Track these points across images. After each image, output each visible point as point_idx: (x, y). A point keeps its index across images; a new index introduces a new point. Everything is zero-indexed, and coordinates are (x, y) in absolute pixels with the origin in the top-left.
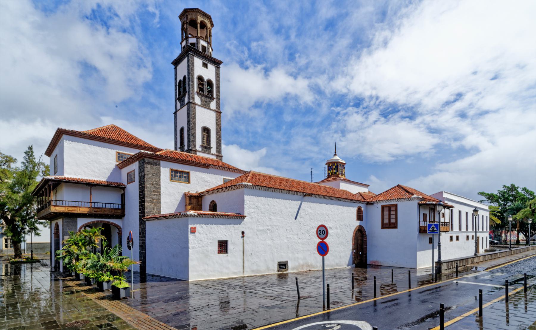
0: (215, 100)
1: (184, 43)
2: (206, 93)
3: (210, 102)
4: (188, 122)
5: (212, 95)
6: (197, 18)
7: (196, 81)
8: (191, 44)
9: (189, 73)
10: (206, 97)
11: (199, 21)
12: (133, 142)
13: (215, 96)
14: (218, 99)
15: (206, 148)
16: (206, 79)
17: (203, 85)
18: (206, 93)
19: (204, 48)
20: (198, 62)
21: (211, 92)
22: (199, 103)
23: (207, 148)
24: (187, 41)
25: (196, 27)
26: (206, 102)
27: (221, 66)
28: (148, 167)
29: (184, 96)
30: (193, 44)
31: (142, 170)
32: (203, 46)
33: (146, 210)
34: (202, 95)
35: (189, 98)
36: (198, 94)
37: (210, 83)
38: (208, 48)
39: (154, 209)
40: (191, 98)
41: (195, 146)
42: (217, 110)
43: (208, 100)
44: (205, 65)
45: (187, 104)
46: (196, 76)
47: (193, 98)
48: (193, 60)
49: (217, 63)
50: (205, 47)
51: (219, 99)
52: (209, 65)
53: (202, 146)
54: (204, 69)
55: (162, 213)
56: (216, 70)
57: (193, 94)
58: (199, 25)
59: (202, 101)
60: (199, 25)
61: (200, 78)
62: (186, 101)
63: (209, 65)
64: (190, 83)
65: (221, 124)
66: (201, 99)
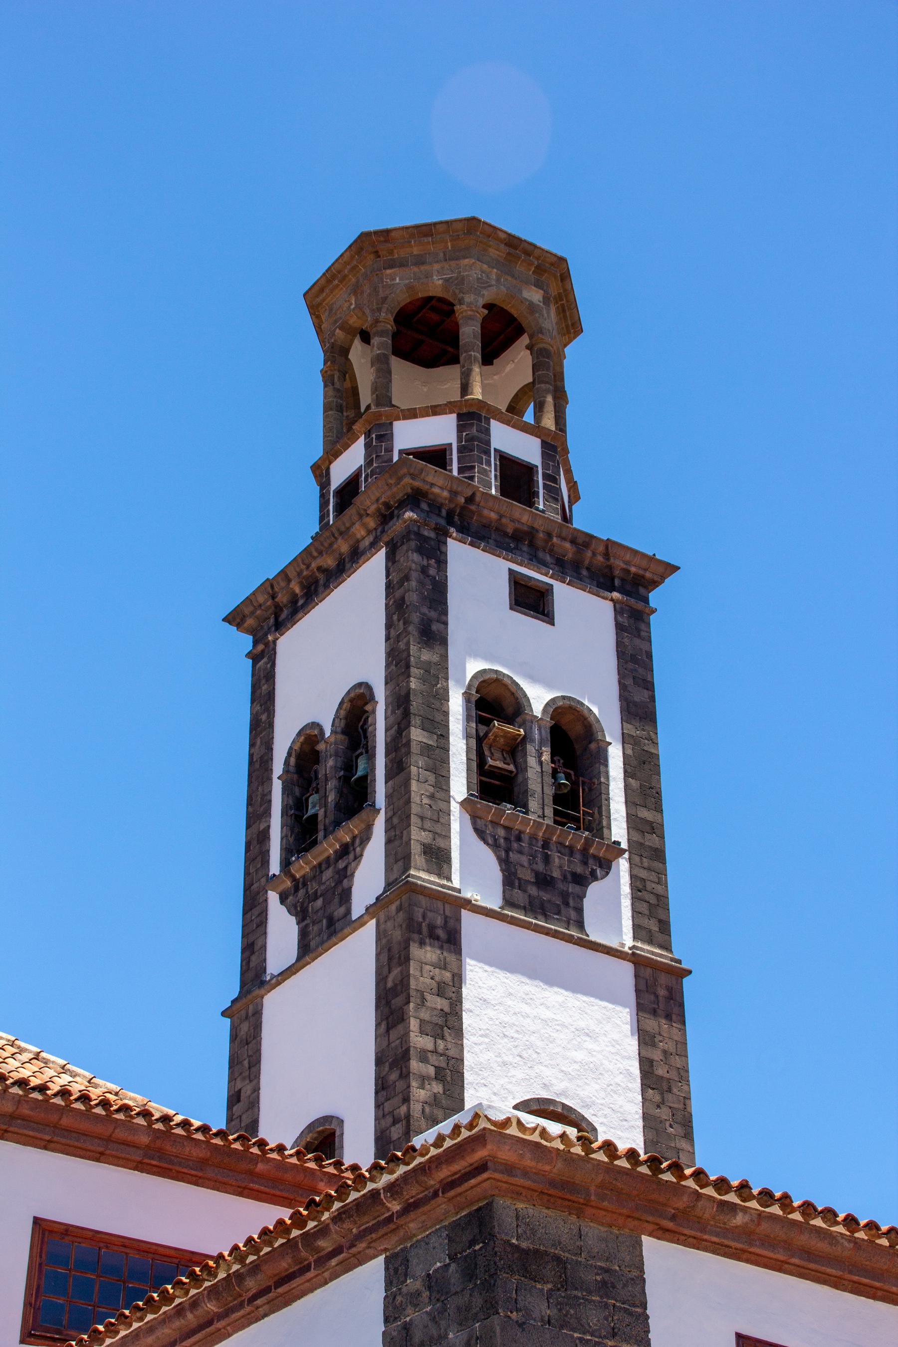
0: (623, 865)
1: (351, 460)
3: (582, 881)
4: (392, 1064)
5: (598, 825)
9: (397, 662)
13: (619, 830)
14: (649, 851)
16: (538, 698)
17: (515, 749)
20: (475, 576)
21: (578, 798)
24: (380, 437)
26: (544, 881)
27: (655, 597)
29: (350, 853)
30: (436, 456)
32: (507, 463)
35: (398, 857)
38: (552, 479)
40: (418, 858)
42: (647, 950)
44: (531, 600)
45: (370, 911)
47: (439, 858)
49: (628, 582)
50: (529, 469)
51: (659, 855)
57: (439, 818)
59: (510, 880)
62: (369, 879)
63: (566, 596)
64: (417, 735)
65: (683, 1074)
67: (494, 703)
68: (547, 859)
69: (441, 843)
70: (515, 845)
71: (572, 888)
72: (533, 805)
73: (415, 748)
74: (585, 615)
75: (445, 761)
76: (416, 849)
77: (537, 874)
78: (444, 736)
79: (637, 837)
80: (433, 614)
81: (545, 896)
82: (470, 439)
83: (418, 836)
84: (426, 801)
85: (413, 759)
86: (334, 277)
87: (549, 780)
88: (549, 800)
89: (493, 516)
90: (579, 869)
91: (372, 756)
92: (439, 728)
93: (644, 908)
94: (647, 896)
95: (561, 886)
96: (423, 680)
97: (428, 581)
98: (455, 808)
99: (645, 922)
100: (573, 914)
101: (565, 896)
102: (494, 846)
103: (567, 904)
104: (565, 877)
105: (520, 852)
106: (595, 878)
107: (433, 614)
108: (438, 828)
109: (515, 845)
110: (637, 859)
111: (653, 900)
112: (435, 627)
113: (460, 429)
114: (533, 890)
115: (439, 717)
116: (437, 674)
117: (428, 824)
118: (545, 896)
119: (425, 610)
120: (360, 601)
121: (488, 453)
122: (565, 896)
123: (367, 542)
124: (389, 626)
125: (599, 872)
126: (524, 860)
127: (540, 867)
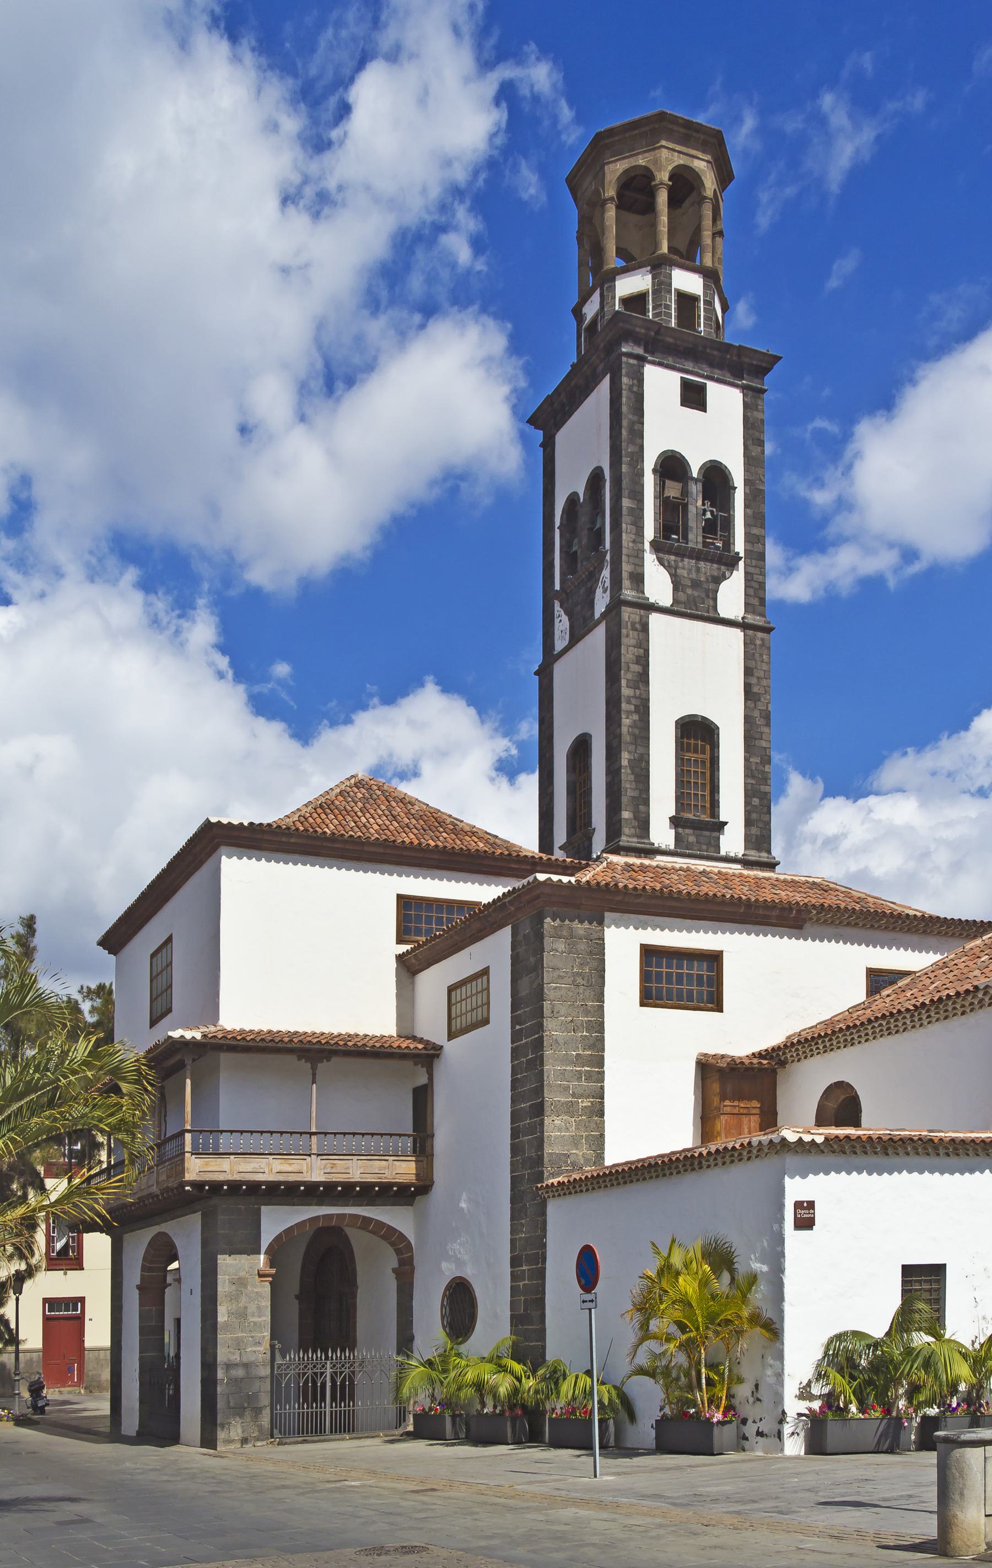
2: (695, 539)
5: (728, 542)
6: (656, 161)
8: (626, 301)
10: (697, 556)
11: (663, 176)
12: (445, 840)
15: (697, 826)
18: (695, 539)
22: (666, 599)
23: (699, 825)
25: (650, 208)
28: (556, 952)
31: (527, 965)
33: (548, 1150)
34: (681, 553)
39: (575, 1142)
41: (644, 825)
53: (675, 822)
55: (608, 1162)
58: (662, 198)
60: (662, 198)
67: (672, 466)
68: (698, 570)
70: (680, 564)
71: (711, 586)
77: (692, 580)
81: (696, 594)
82: (660, 283)
89: (671, 340)
95: (705, 586)
100: (711, 603)
103: (708, 596)
104: (707, 580)
105: (683, 568)
106: (725, 578)
113: (653, 278)
114: (689, 591)
118: (696, 594)
122: (707, 591)
125: (727, 574)
127: (694, 576)
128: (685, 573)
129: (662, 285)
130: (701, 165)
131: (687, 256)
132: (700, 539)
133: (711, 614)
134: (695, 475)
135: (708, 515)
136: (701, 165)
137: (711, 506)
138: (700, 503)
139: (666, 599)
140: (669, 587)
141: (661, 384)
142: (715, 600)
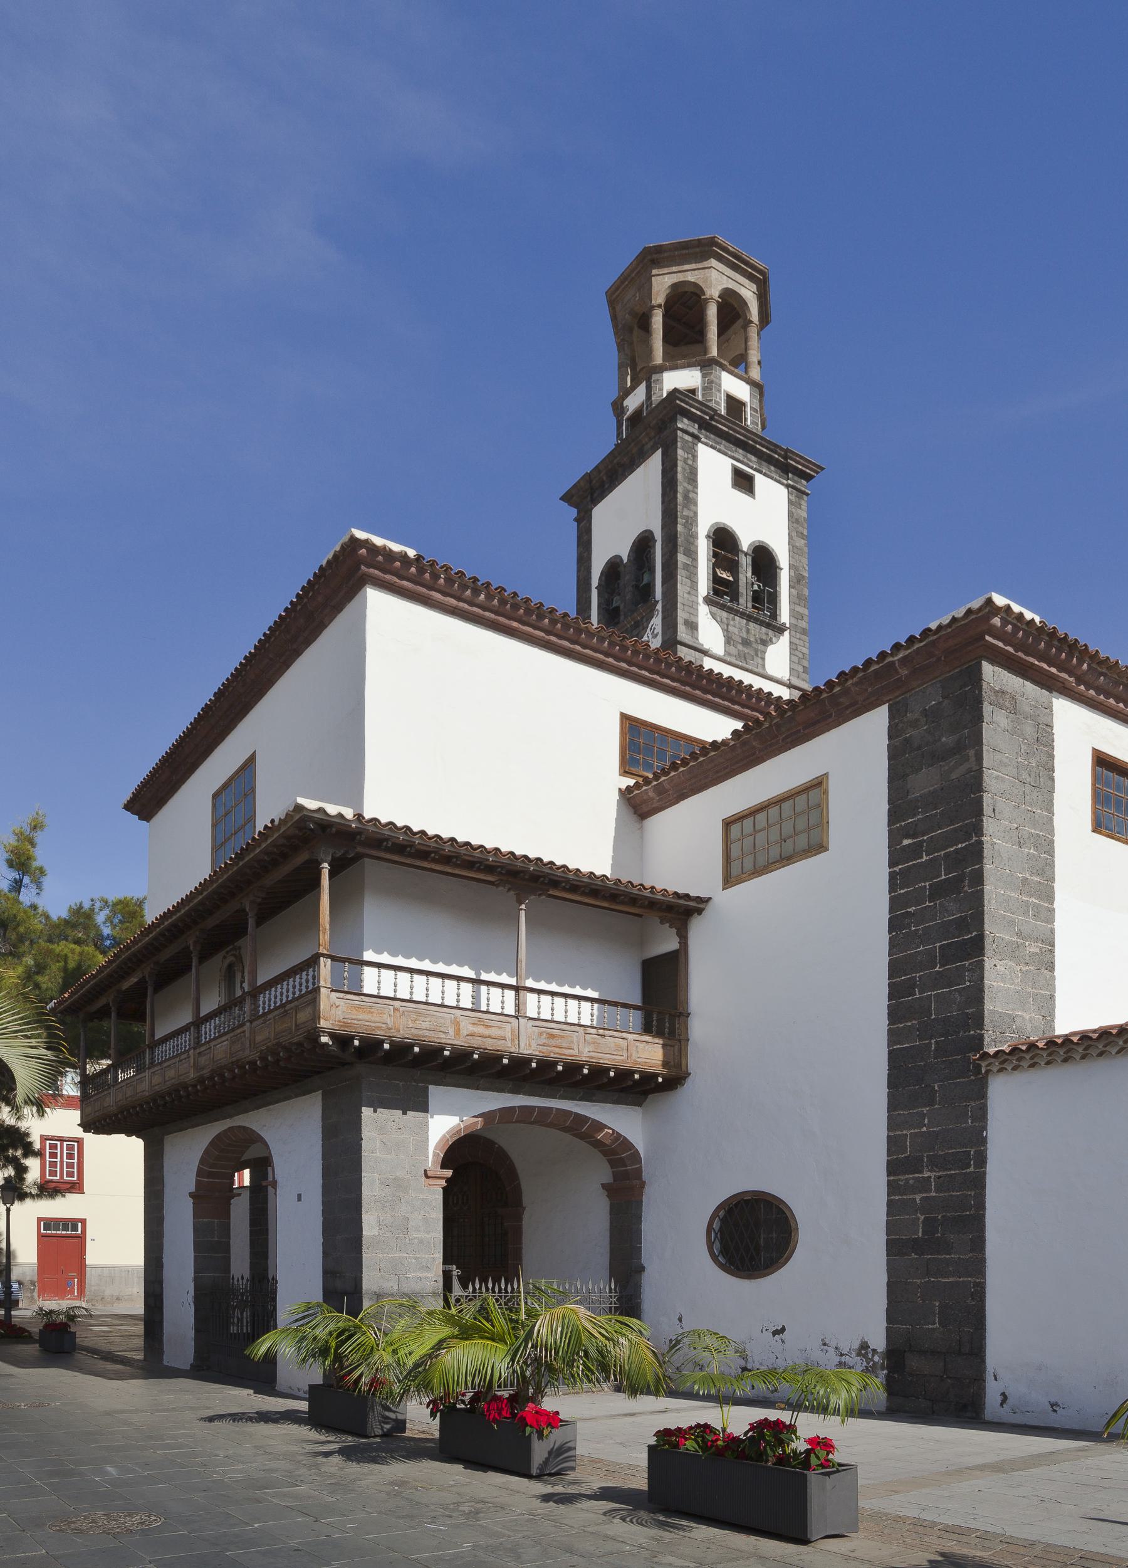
2: (745, 602)
3: (765, 643)
5: (774, 615)
7: (703, 548)
13: (784, 617)
17: (733, 567)
19: (735, 405)
20: (713, 466)
21: (765, 599)
22: (719, 650)
26: (746, 643)
32: (730, 399)
36: (708, 601)
37: (763, 558)
40: (681, 628)
43: (757, 631)
46: (703, 529)
47: (693, 626)
48: (695, 457)
50: (743, 404)
52: (760, 481)
54: (741, 497)
56: (790, 502)
59: (729, 640)
61: (723, 539)
64: (681, 558)
66: (726, 631)
68: (748, 631)
69: (693, 619)
70: (732, 623)
71: (760, 647)
72: (742, 600)
73: (680, 565)
74: (772, 493)
75: (696, 574)
76: (680, 621)
77: (743, 639)
78: (695, 560)
79: (794, 621)
80: (690, 487)
83: (681, 615)
84: (686, 595)
85: (679, 571)
86: (625, 279)
87: (749, 586)
88: (750, 599)
90: (764, 637)
91: (652, 570)
92: (692, 554)
93: (796, 659)
94: (797, 653)
95: (754, 645)
96: (684, 525)
97: (687, 467)
98: (701, 600)
99: (796, 667)
100: (760, 661)
101: (756, 651)
102: (720, 622)
103: (757, 655)
107: (690, 487)
108: (691, 611)
109: (732, 623)
110: (793, 633)
111: (801, 655)
112: (691, 495)
113: (704, 376)
114: (740, 647)
115: (692, 548)
116: (692, 521)
117: (686, 608)
119: (686, 485)
120: (647, 477)
121: (720, 391)
122: (756, 651)
123: (649, 446)
124: (664, 495)
125: (774, 640)
126: (736, 631)
127: (744, 635)
128: (736, 631)
129: (710, 386)
130: (748, 292)
131: (738, 363)
132: (750, 605)
133: (760, 670)
134: (745, 549)
135: (756, 587)
136: (748, 292)
137: (758, 580)
138: (749, 574)
139: (719, 650)
140: (722, 640)
141: (713, 466)
142: (763, 659)
